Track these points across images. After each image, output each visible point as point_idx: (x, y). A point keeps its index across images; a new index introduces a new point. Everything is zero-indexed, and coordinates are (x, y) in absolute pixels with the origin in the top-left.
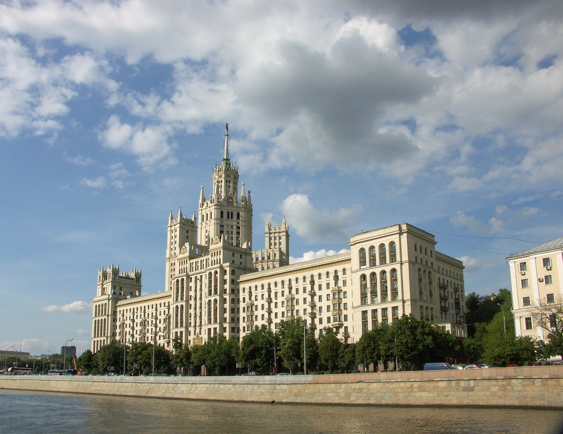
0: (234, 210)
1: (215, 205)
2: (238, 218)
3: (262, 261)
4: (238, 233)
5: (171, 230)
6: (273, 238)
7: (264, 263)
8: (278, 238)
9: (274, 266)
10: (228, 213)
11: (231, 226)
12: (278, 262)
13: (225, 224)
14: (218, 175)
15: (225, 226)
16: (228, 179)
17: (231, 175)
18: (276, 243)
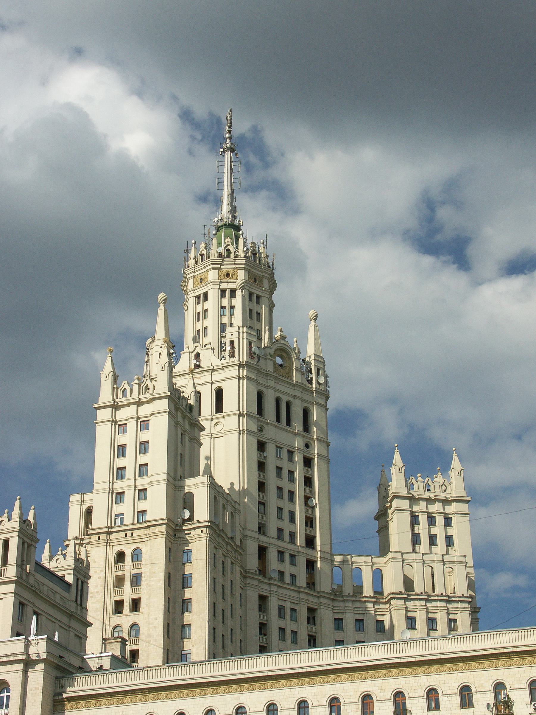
0: (294, 397)
1: (240, 366)
2: (307, 428)
3: (377, 598)
4: (308, 481)
5: (114, 422)
6: (423, 519)
7: (412, 602)
8: (440, 520)
9: (451, 617)
10: (278, 401)
11: (289, 451)
12: (467, 605)
13: (273, 440)
14: (220, 269)
15: (271, 449)
16: (256, 291)
17: (263, 277)
18: (435, 536)
